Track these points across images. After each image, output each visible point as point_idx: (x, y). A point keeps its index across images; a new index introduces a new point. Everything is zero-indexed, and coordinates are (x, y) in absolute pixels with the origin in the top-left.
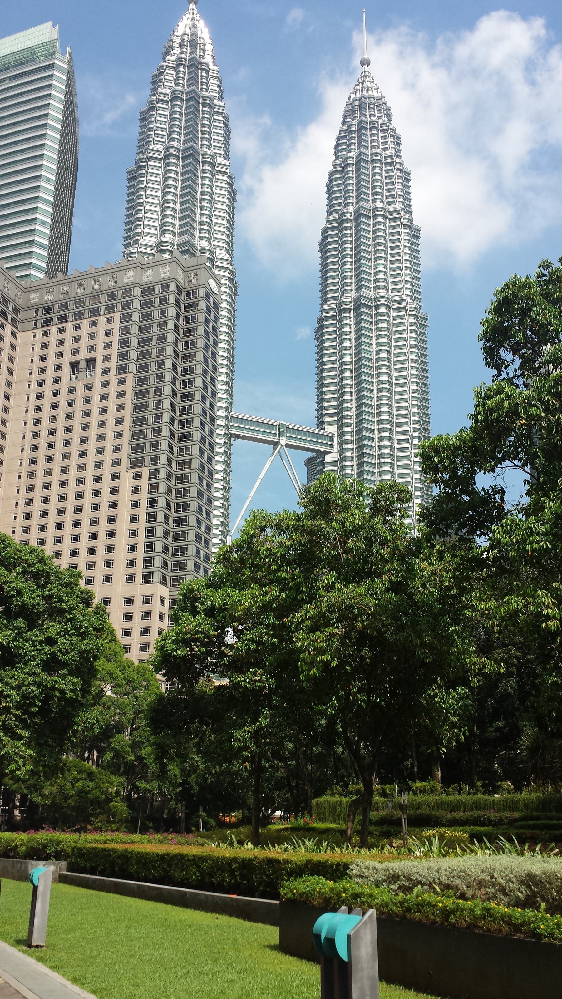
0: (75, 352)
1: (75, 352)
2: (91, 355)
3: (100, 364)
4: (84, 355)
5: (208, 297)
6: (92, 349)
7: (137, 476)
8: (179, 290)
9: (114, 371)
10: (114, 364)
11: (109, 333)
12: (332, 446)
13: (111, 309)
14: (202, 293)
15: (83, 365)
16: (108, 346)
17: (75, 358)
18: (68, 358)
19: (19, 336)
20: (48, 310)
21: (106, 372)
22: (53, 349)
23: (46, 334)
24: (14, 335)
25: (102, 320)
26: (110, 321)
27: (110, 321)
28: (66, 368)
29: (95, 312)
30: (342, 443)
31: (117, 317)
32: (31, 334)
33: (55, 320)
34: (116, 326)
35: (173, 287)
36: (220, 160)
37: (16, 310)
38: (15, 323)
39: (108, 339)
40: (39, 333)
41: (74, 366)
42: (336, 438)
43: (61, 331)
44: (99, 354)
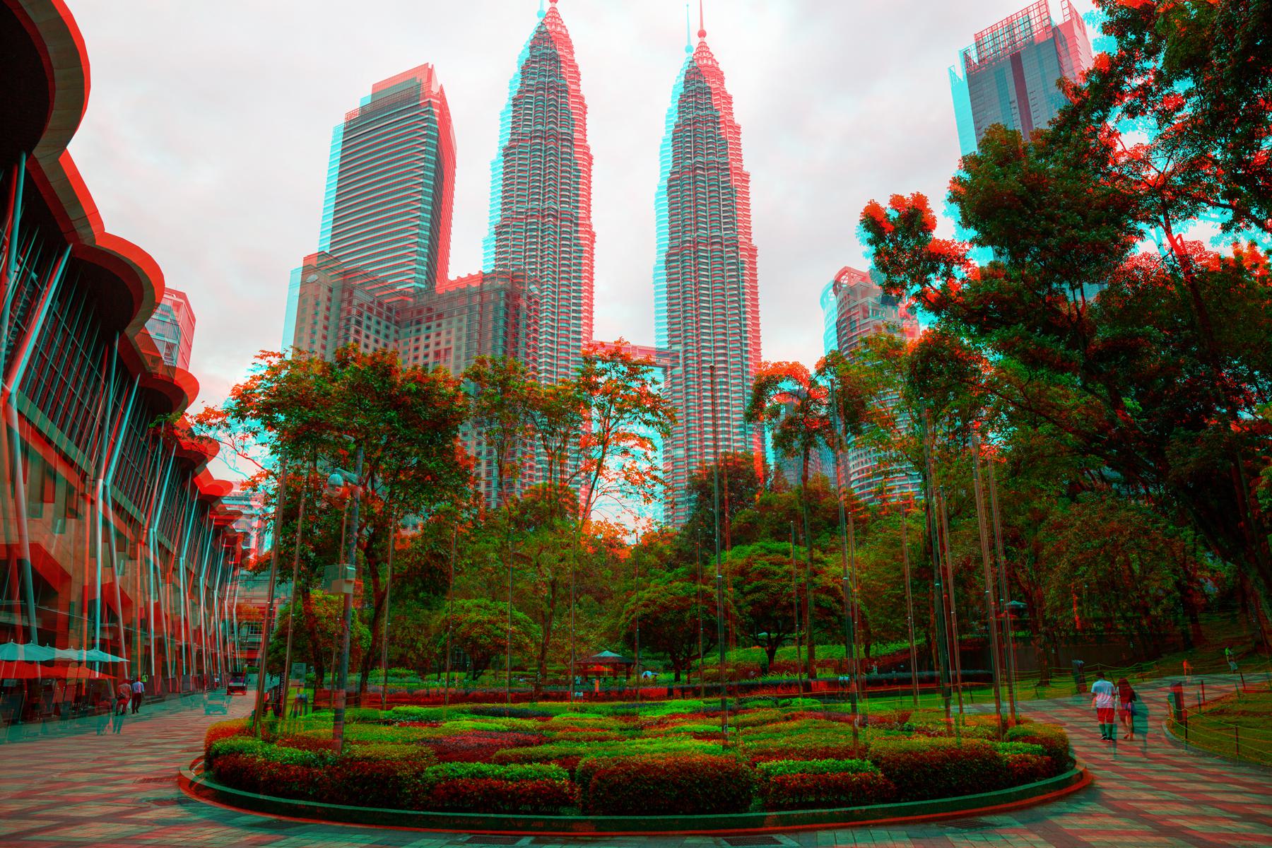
0: (438, 344)
1: (438, 344)
2: (448, 346)
3: (453, 350)
4: (443, 346)
6: (448, 341)
8: (507, 296)
13: (461, 313)
18: (432, 348)
20: (420, 312)
21: (458, 357)
24: (397, 332)
25: (455, 320)
26: (461, 320)
27: (461, 320)
29: (451, 315)
30: (686, 359)
31: (465, 318)
33: (424, 320)
35: (503, 295)
37: (397, 313)
38: (397, 323)
41: (437, 354)
42: (681, 355)
44: (453, 343)
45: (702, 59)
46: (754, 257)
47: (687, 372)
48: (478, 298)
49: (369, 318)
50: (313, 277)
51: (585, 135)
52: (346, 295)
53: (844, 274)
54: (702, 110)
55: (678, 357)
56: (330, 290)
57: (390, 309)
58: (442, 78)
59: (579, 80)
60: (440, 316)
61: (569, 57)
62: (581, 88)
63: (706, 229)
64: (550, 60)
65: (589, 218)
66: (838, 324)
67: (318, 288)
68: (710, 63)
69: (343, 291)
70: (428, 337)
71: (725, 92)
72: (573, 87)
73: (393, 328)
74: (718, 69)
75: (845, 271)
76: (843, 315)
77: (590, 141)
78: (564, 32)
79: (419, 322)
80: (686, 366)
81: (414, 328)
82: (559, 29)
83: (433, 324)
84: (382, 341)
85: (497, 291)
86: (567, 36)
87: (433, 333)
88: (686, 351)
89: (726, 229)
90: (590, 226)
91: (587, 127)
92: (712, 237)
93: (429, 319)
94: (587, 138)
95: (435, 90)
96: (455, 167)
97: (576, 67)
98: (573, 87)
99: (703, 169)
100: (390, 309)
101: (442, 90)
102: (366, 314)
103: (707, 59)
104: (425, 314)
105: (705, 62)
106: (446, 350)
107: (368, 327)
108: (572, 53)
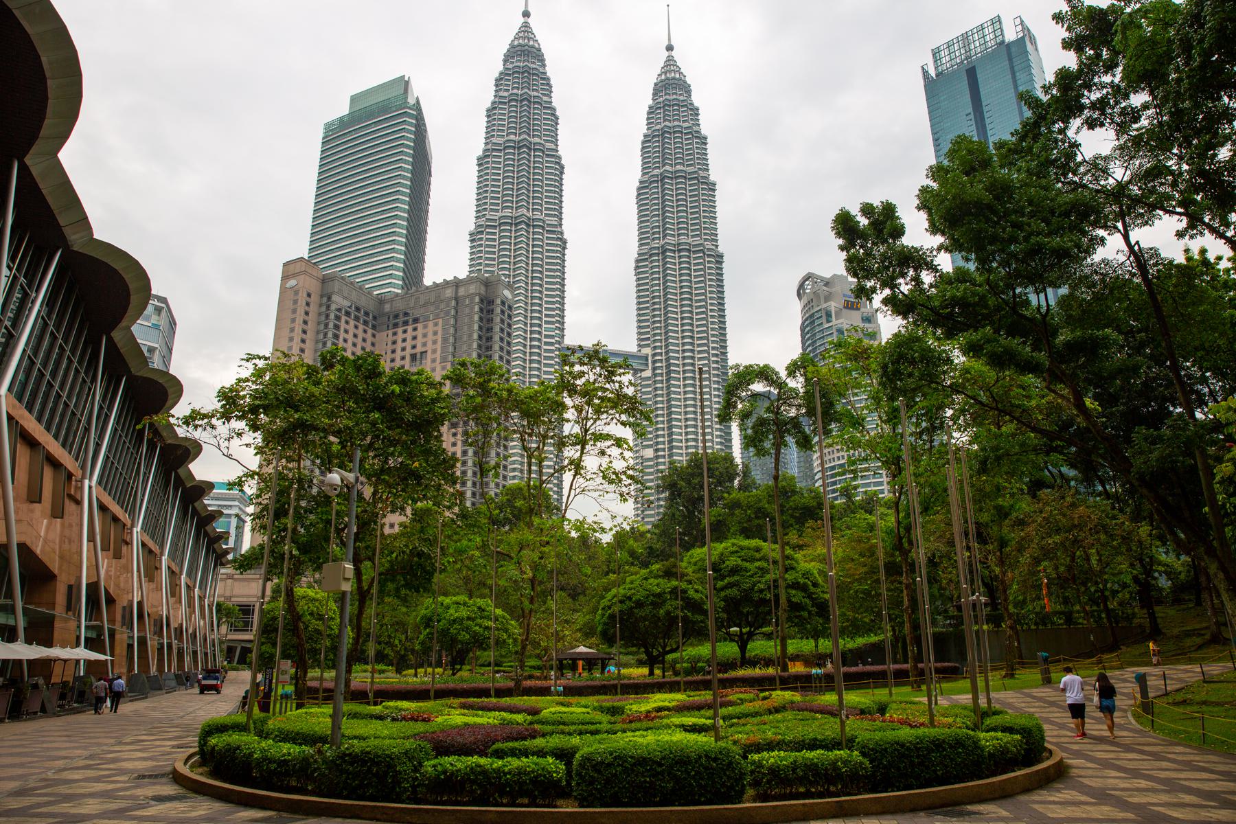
0: (414, 347)
1: (414, 347)
2: (424, 349)
3: (429, 354)
4: (419, 349)
5: (503, 303)
6: (424, 344)
7: (455, 435)
8: (482, 301)
9: (438, 361)
10: (438, 355)
11: (435, 333)
12: (647, 365)
13: (437, 317)
14: (498, 301)
15: (418, 356)
16: (435, 342)
17: (414, 351)
18: (409, 351)
19: (377, 336)
20: (396, 316)
21: (434, 361)
22: (400, 345)
23: (395, 334)
24: (374, 336)
25: (431, 324)
26: (436, 325)
27: (436, 325)
28: (408, 358)
29: (427, 319)
30: (654, 362)
31: (440, 321)
32: (385, 334)
33: (401, 324)
34: (439, 329)
35: (477, 299)
36: (548, 145)
37: (375, 318)
38: (374, 327)
39: (435, 338)
40: (390, 332)
43: (405, 332)
44: (429, 347)
45: (670, 72)
46: (721, 263)
47: (655, 375)
48: (453, 303)
49: (347, 323)
50: (292, 283)
51: (557, 145)
52: (325, 300)
53: (807, 280)
54: (670, 121)
55: (647, 360)
56: (309, 295)
57: (367, 314)
58: (418, 90)
59: (551, 92)
60: (416, 321)
61: (541, 70)
62: (553, 100)
63: (674, 236)
64: (523, 73)
65: (561, 225)
66: (803, 329)
67: (297, 293)
68: (677, 76)
69: (322, 296)
70: (404, 340)
71: (692, 104)
72: (545, 98)
73: (370, 331)
74: (685, 82)
75: (809, 277)
76: (806, 320)
77: (562, 151)
78: (537, 46)
79: (396, 325)
80: (654, 369)
81: (390, 332)
82: (531, 43)
83: (410, 328)
84: (419, 342)
85: (471, 296)
86: (539, 50)
87: (409, 335)
88: (654, 355)
89: (693, 236)
90: (562, 233)
91: (559, 137)
92: (679, 244)
93: (406, 323)
94: (559, 148)
95: (411, 101)
96: (430, 175)
97: (548, 79)
98: (545, 98)
99: (672, 179)
100: (367, 314)
101: (418, 102)
102: (344, 318)
103: (675, 72)
104: (401, 319)
105: (673, 75)
106: (422, 353)
107: (346, 331)
108: (544, 66)
